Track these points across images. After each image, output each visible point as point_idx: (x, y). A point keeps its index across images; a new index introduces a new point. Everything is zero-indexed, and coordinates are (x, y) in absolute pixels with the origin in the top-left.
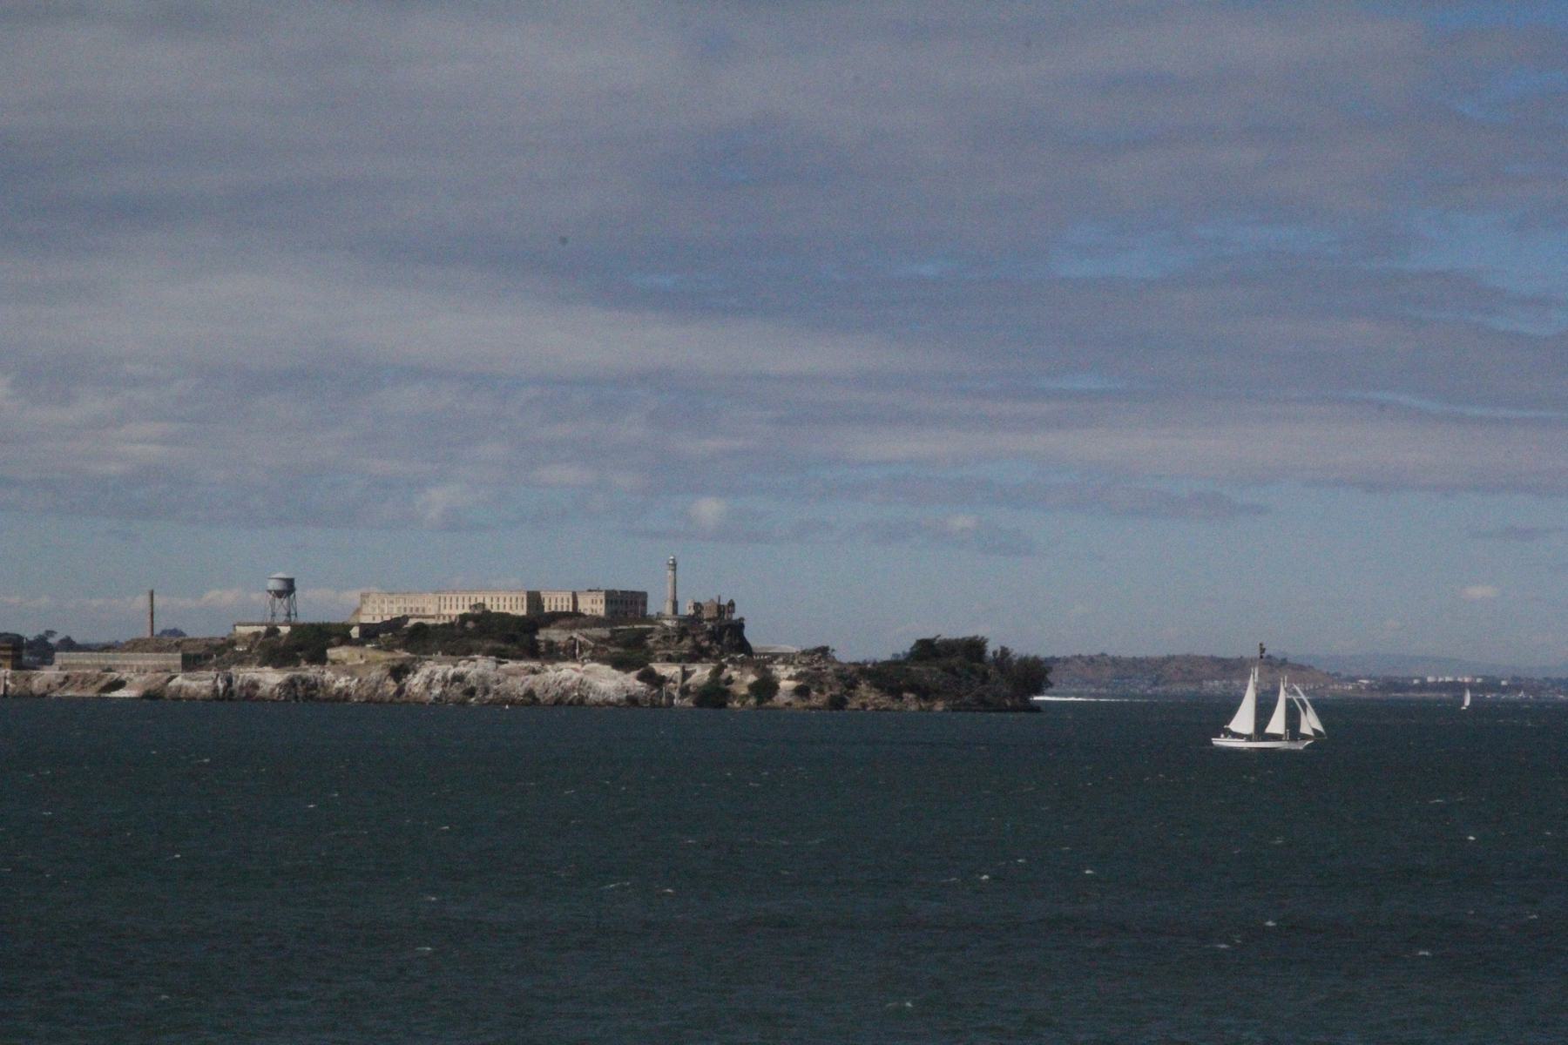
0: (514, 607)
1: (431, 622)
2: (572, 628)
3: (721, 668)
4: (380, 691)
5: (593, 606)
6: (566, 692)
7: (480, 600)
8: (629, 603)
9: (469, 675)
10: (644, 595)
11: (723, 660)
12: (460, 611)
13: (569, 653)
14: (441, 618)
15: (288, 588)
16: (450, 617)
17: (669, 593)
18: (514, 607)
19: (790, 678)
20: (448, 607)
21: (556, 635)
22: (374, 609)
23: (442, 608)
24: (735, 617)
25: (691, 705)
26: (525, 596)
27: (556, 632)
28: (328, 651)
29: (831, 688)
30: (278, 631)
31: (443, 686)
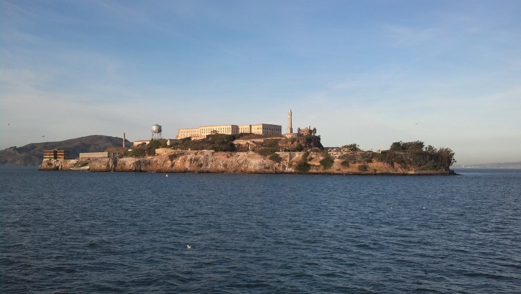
0: (227, 131)
1: (198, 138)
2: (248, 139)
3: (307, 154)
4: (165, 165)
5: (257, 130)
6: (240, 165)
7: (215, 129)
8: (273, 129)
9: (201, 159)
10: (281, 126)
11: (308, 150)
12: (208, 134)
13: (245, 149)
14: (201, 137)
15: (160, 130)
16: (204, 136)
17: (290, 126)
18: (227, 131)
19: (339, 158)
20: (204, 133)
21: (242, 142)
22: (182, 135)
23: (202, 133)
24: (317, 135)
25: (293, 171)
26: (231, 127)
27: (241, 140)
28: (156, 150)
29: (360, 162)
30: (145, 143)
31: (190, 163)
